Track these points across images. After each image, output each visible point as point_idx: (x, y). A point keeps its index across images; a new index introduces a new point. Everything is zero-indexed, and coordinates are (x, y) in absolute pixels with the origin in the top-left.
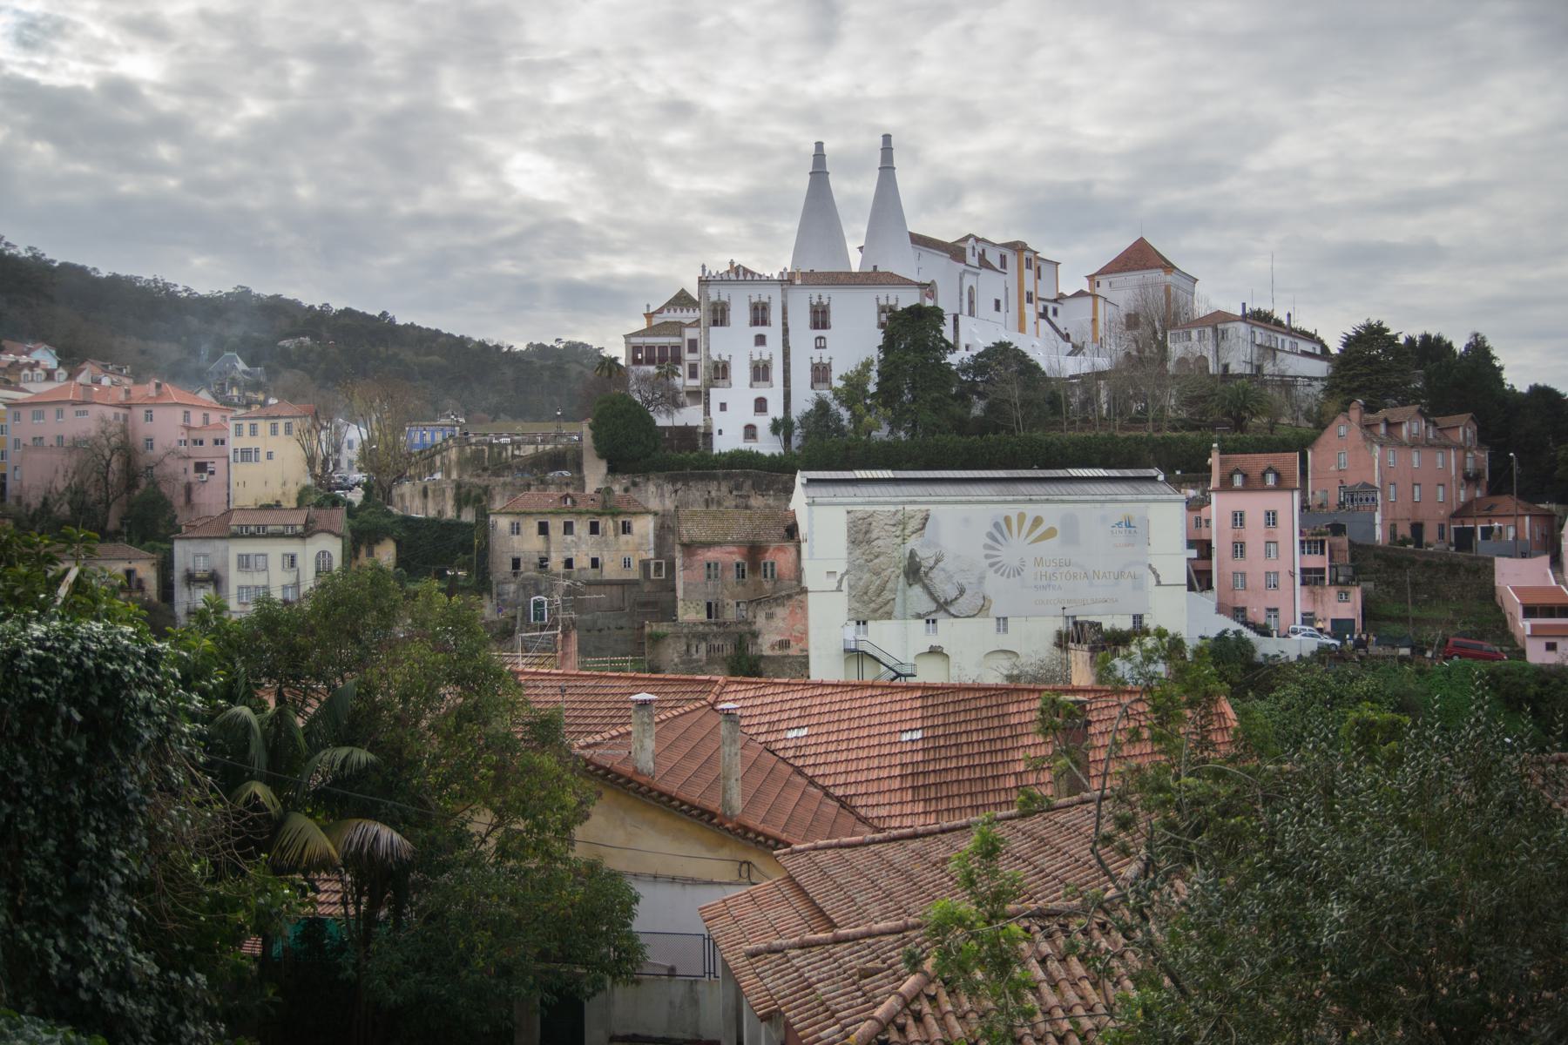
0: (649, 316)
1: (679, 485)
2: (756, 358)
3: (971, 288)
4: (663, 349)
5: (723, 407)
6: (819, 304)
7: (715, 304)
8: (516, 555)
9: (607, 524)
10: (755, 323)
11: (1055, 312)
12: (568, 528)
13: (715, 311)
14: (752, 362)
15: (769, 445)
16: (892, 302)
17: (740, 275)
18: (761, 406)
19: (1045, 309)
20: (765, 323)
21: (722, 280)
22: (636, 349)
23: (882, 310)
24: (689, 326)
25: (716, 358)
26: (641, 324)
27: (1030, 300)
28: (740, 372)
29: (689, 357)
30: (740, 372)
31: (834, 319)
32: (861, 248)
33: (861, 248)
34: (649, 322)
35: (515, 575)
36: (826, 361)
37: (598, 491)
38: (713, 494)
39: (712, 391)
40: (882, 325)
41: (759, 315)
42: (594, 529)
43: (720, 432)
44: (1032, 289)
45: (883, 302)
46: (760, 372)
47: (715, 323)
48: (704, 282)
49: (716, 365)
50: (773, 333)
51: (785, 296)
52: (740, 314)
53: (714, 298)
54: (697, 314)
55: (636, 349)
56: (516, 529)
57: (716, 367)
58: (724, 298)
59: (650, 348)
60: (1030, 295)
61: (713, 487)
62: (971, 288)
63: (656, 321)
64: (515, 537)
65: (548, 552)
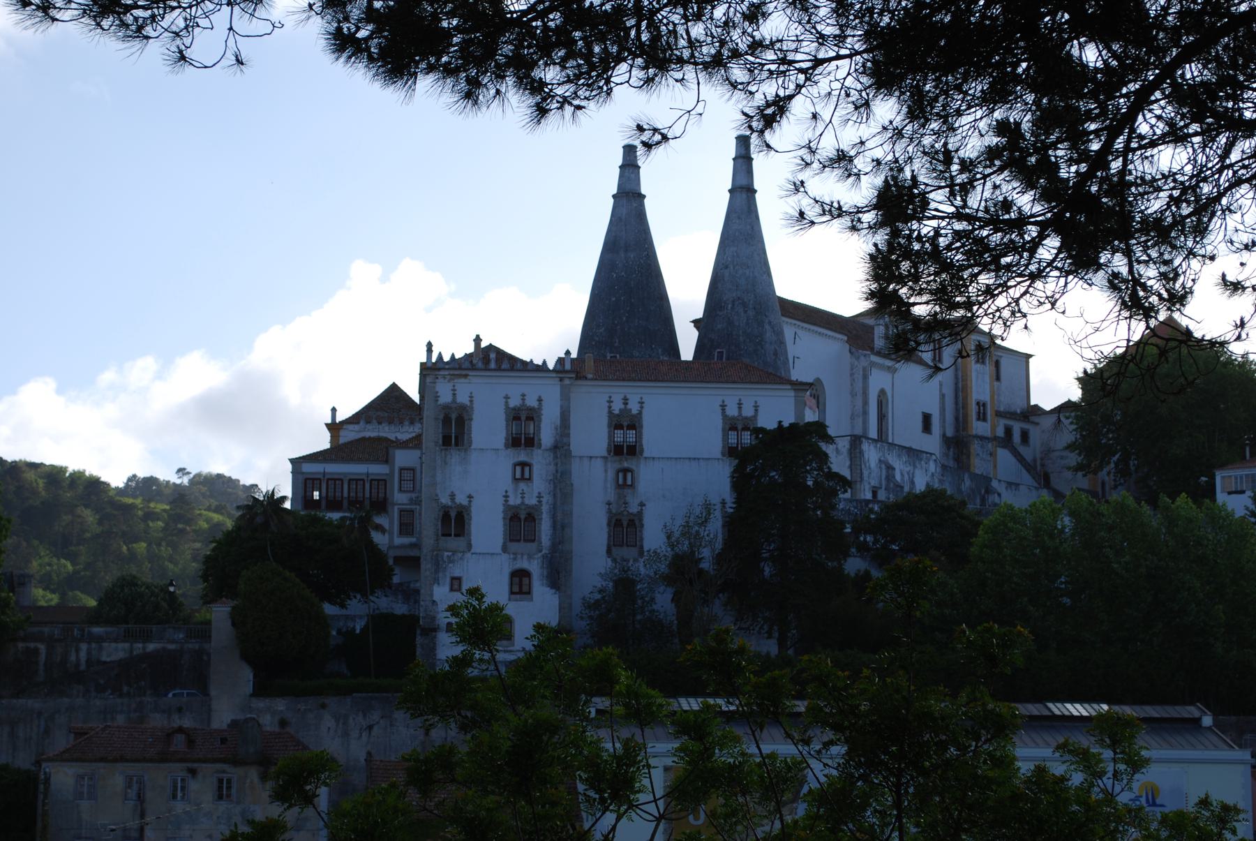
0: (334, 427)
2: (514, 501)
3: (882, 393)
4: (356, 481)
6: (625, 411)
7: (446, 408)
11: (1025, 436)
13: (446, 421)
14: (507, 507)
16: (748, 412)
17: (488, 360)
18: (520, 582)
19: (1008, 431)
20: (531, 442)
21: (460, 367)
23: (732, 425)
24: (404, 445)
25: (445, 500)
26: (323, 442)
27: (982, 417)
28: (487, 527)
29: (400, 498)
30: (487, 527)
32: (696, 323)
33: (696, 323)
34: (334, 438)
36: (634, 509)
37: (234, 724)
40: (731, 452)
41: (522, 430)
44: (985, 397)
45: (732, 411)
46: (520, 524)
48: (431, 371)
51: (565, 397)
52: (488, 429)
53: (445, 397)
54: (416, 429)
57: (446, 517)
58: (463, 398)
59: (335, 480)
60: (981, 405)
62: (882, 393)
63: (348, 436)
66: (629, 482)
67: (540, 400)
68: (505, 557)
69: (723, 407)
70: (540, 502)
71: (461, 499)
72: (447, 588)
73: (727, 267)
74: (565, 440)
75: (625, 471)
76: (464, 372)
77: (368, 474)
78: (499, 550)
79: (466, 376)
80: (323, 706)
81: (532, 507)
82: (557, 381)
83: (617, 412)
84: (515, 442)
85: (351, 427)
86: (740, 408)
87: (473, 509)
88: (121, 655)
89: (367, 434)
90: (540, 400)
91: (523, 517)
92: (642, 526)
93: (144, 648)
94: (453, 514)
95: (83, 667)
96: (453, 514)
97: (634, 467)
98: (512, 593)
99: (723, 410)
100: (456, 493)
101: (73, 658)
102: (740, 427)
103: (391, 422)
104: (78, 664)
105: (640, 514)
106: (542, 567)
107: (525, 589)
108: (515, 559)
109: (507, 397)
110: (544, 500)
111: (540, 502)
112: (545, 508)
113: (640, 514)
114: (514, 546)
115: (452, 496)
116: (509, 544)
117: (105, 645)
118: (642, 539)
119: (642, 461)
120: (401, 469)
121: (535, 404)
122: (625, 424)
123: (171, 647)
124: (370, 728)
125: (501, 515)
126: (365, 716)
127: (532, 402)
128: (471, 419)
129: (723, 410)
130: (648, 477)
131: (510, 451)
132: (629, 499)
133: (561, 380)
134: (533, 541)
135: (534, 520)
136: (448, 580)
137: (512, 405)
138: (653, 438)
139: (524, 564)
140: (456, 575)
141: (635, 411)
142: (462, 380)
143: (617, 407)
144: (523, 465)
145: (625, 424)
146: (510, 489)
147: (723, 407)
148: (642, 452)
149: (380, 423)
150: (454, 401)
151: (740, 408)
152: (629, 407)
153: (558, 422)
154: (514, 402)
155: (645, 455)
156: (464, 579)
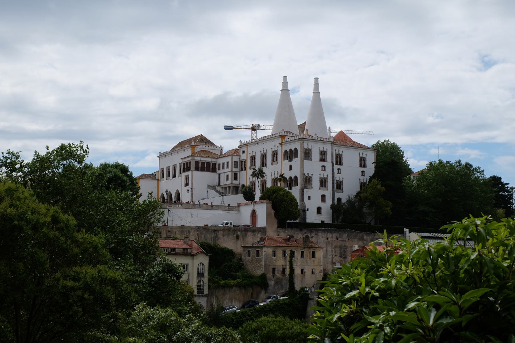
1: (313, 234)
2: (322, 176)
4: (208, 164)
5: (309, 198)
7: (306, 149)
8: (274, 267)
9: (306, 252)
10: (321, 160)
12: (292, 254)
13: (305, 153)
15: (326, 217)
18: (323, 198)
22: (197, 163)
25: (306, 175)
28: (316, 183)
30: (316, 183)
31: (344, 160)
35: (273, 276)
36: (341, 180)
38: (329, 239)
39: (305, 190)
42: (302, 255)
45: (361, 156)
46: (323, 183)
47: (305, 159)
49: (307, 177)
50: (328, 165)
52: (316, 155)
53: (306, 147)
55: (197, 163)
56: (274, 254)
57: (306, 180)
61: (329, 235)
64: (274, 258)
65: (286, 265)
71: (310, 175)
84: (321, 160)
113: (342, 181)
115: (308, 174)
116: (321, 188)
120: (235, 162)
121: (326, 150)
124: (312, 237)
127: (325, 150)
143: (337, 152)
144: (323, 166)
154: (321, 149)
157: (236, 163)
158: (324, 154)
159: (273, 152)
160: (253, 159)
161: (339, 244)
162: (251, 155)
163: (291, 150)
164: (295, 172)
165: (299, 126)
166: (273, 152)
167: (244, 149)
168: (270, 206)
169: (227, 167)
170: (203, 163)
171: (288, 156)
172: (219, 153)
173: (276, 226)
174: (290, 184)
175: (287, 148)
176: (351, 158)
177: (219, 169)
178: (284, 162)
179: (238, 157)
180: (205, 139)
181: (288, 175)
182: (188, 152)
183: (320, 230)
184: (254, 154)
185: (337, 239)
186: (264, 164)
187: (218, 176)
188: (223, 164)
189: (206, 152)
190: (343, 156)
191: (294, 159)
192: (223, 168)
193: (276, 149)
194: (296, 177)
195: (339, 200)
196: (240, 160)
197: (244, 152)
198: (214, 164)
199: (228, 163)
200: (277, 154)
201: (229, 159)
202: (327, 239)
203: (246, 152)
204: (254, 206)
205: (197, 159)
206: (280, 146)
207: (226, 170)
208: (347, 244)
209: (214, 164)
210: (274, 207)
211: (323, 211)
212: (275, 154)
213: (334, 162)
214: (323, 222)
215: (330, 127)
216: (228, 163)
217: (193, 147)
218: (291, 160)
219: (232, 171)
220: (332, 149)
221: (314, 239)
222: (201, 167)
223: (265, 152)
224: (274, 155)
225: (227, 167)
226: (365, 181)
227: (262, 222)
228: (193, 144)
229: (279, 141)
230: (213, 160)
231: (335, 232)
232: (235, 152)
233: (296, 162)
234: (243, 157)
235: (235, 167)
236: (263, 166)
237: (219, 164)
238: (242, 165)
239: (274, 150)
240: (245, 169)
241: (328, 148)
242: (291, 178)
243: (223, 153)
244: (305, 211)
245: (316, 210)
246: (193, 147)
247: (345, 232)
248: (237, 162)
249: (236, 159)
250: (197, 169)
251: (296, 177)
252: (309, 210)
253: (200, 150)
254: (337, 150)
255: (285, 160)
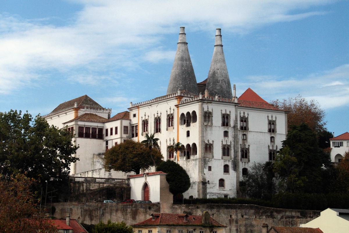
1: (215, 211)
2: (224, 143)
4: (94, 129)
6: (244, 116)
7: (206, 113)
18: (226, 169)
20: (227, 125)
22: (81, 128)
25: (206, 142)
28: (218, 151)
30: (218, 151)
36: (247, 147)
38: (234, 217)
43: (208, 181)
45: (270, 119)
46: (226, 150)
49: (206, 144)
52: (217, 120)
53: (206, 110)
55: (81, 128)
58: (210, 110)
61: (233, 212)
66: (245, 139)
67: (230, 112)
68: (222, 160)
69: (268, 117)
70: (231, 144)
71: (211, 142)
72: (208, 170)
73: (218, 69)
74: (236, 125)
75: (244, 135)
76: (211, 102)
77: (97, 126)
78: (221, 159)
79: (211, 103)
80: (198, 208)
81: (229, 145)
82: (234, 107)
83: (242, 116)
85: (82, 109)
86: (272, 118)
87: (214, 145)
88: (96, 187)
89: (87, 112)
90: (230, 112)
91: (226, 148)
92: (249, 152)
93: (103, 185)
94: (208, 146)
95: (85, 191)
96: (208, 146)
97: (246, 134)
98: (224, 172)
99: (268, 118)
100: (209, 140)
101: (81, 188)
102: (272, 123)
103: (94, 109)
104: (83, 190)
105: (249, 148)
106: (232, 164)
107: (227, 171)
108: (225, 161)
109: (221, 110)
110: (232, 143)
111: (231, 144)
112: (232, 146)
113: (248, 149)
114: (224, 157)
115: (208, 141)
117: (91, 184)
118: (249, 156)
119: (249, 132)
120: (125, 127)
122: (244, 120)
123: (111, 185)
124: (213, 215)
125: (221, 147)
126: (211, 211)
127: (228, 113)
128: (212, 117)
129: (268, 118)
130: (251, 137)
131: (223, 127)
132: (246, 144)
133: (235, 106)
134: (229, 156)
135: (229, 149)
136: (208, 167)
137: (223, 113)
138: (251, 126)
139: (227, 163)
140: (210, 166)
141: (246, 117)
142: (210, 104)
143: (242, 115)
145: (244, 120)
146: (223, 139)
147: (268, 117)
148: (248, 129)
149: (91, 109)
150: (208, 111)
151: (272, 118)
152: (245, 115)
153: (235, 119)
154: (224, 112)
155: (249, 130)
156: (212, 167)
157: (126, 128)
158: (227, 117)
159: (168, 115)
160: (145, 123)
161: (244, 222)
162: (143, 119)
163: (188, 113)
164: (195, 139)
165: (198, 84)
166: (168, 115)
167: (135, 111)
168: (164, 177)
169: (116, 133)
170: (88, 128)
171: (185, 121)
172: (107, 118)
173: (172, 202)
174: (188, 153)
175: (185, 110)
176: (258, 121)
177: (107, 135)
178: (180, 127)
179: (128, 122)
180: (91, 100)
181: (184, 141)
182: (71, 115)
183: (223, 206)
184: (147, 118)
185: (242, 216)
186: (158, 130)
187: (105, 143)
188: (112, 129)
189: (91, 114)
190: (250, 120)
191: (192, 124)
192: (111, 134)
193: (172, 112)
194: (194, 145)
195: (245, 171)
196: (130, 124)
197: (135, 116)
198: (101, 130)
199: (116, 128)
200: (173, 118)
201: (117, 124)
202: (231, 216)
203: (137, 115)
204: (146, 179)
205: (81, 123)
206: (176, 108)
207: (114, 136)
208: (254, 223)
209: (101, 130)
210: (168, 180)
211: (227, 183)
212: (170, 118)
213: (239, 127)
214: (226, 196)
215: (235, 85)
216: (116, 128)
217: (77, 110)
218: (188, 125)
219: (121, 138)
220: (236, 111)
221: (215, 217)
222: (84, 133)
223: (159, 115)
224: (169, 119)
225: (116, 133)
226: (275, 148)
227: (155, 197)
228: (75, 106)
229: (176, 102)
230: (100, 125)
231: (239, 209)
232: (125, 116)
233: (195, 128)
234: (134, 121)
235: (125, 133)
236: (157, 132)
237: (107, 130)
238: (133, 130)
239: (169, 113)
240: (137, 136)
241: (231, 110)
242: (188, 145)
243: (111, 117)
244: (204, 183)
245: (218, 183)
246: (77, 110)
247: (251, 208)
248: (127, 127)
249: (126, 123)
250: (81, 135)
251: (194, 145)
252: (210, 181)
253: (85, 113)
254: (242, 112)
255: (181, 124)
